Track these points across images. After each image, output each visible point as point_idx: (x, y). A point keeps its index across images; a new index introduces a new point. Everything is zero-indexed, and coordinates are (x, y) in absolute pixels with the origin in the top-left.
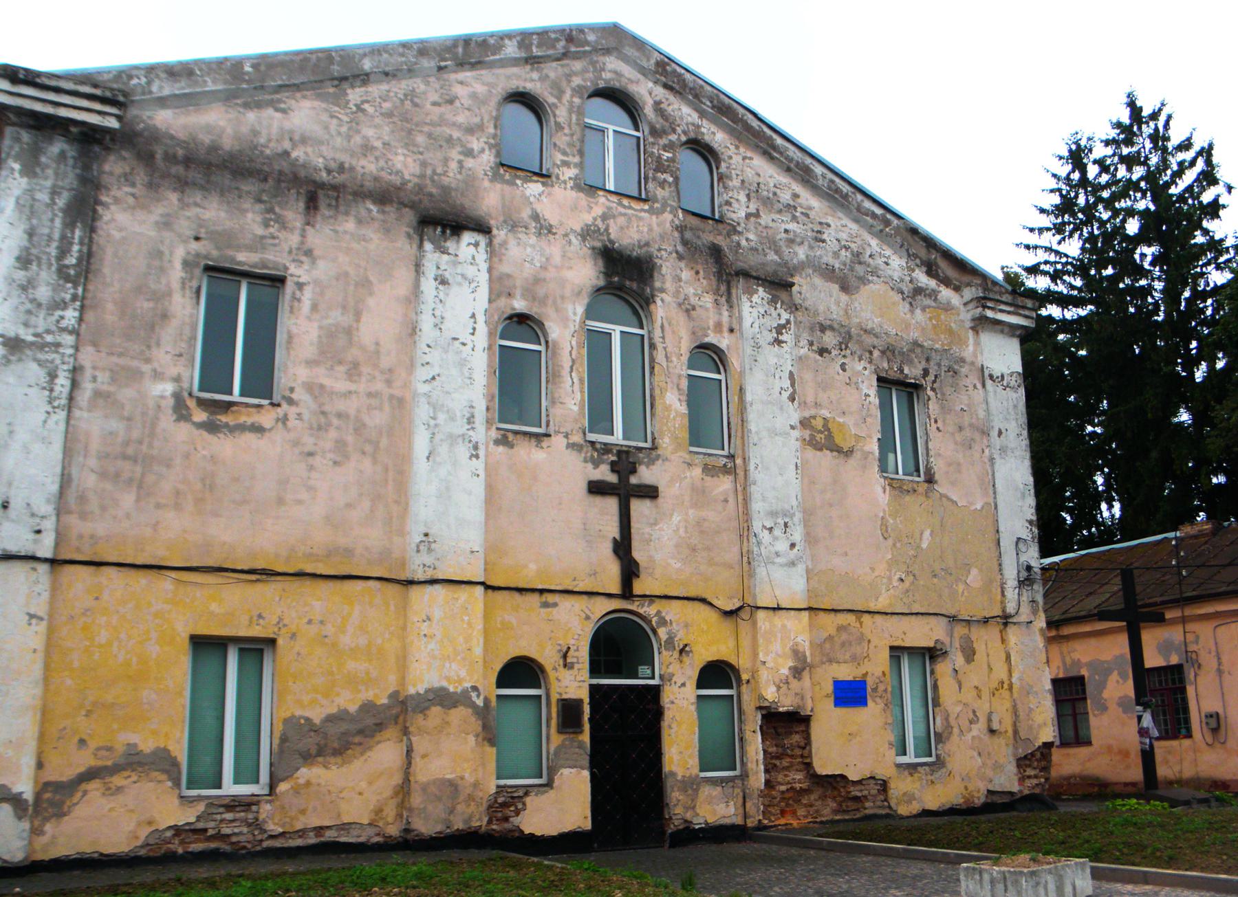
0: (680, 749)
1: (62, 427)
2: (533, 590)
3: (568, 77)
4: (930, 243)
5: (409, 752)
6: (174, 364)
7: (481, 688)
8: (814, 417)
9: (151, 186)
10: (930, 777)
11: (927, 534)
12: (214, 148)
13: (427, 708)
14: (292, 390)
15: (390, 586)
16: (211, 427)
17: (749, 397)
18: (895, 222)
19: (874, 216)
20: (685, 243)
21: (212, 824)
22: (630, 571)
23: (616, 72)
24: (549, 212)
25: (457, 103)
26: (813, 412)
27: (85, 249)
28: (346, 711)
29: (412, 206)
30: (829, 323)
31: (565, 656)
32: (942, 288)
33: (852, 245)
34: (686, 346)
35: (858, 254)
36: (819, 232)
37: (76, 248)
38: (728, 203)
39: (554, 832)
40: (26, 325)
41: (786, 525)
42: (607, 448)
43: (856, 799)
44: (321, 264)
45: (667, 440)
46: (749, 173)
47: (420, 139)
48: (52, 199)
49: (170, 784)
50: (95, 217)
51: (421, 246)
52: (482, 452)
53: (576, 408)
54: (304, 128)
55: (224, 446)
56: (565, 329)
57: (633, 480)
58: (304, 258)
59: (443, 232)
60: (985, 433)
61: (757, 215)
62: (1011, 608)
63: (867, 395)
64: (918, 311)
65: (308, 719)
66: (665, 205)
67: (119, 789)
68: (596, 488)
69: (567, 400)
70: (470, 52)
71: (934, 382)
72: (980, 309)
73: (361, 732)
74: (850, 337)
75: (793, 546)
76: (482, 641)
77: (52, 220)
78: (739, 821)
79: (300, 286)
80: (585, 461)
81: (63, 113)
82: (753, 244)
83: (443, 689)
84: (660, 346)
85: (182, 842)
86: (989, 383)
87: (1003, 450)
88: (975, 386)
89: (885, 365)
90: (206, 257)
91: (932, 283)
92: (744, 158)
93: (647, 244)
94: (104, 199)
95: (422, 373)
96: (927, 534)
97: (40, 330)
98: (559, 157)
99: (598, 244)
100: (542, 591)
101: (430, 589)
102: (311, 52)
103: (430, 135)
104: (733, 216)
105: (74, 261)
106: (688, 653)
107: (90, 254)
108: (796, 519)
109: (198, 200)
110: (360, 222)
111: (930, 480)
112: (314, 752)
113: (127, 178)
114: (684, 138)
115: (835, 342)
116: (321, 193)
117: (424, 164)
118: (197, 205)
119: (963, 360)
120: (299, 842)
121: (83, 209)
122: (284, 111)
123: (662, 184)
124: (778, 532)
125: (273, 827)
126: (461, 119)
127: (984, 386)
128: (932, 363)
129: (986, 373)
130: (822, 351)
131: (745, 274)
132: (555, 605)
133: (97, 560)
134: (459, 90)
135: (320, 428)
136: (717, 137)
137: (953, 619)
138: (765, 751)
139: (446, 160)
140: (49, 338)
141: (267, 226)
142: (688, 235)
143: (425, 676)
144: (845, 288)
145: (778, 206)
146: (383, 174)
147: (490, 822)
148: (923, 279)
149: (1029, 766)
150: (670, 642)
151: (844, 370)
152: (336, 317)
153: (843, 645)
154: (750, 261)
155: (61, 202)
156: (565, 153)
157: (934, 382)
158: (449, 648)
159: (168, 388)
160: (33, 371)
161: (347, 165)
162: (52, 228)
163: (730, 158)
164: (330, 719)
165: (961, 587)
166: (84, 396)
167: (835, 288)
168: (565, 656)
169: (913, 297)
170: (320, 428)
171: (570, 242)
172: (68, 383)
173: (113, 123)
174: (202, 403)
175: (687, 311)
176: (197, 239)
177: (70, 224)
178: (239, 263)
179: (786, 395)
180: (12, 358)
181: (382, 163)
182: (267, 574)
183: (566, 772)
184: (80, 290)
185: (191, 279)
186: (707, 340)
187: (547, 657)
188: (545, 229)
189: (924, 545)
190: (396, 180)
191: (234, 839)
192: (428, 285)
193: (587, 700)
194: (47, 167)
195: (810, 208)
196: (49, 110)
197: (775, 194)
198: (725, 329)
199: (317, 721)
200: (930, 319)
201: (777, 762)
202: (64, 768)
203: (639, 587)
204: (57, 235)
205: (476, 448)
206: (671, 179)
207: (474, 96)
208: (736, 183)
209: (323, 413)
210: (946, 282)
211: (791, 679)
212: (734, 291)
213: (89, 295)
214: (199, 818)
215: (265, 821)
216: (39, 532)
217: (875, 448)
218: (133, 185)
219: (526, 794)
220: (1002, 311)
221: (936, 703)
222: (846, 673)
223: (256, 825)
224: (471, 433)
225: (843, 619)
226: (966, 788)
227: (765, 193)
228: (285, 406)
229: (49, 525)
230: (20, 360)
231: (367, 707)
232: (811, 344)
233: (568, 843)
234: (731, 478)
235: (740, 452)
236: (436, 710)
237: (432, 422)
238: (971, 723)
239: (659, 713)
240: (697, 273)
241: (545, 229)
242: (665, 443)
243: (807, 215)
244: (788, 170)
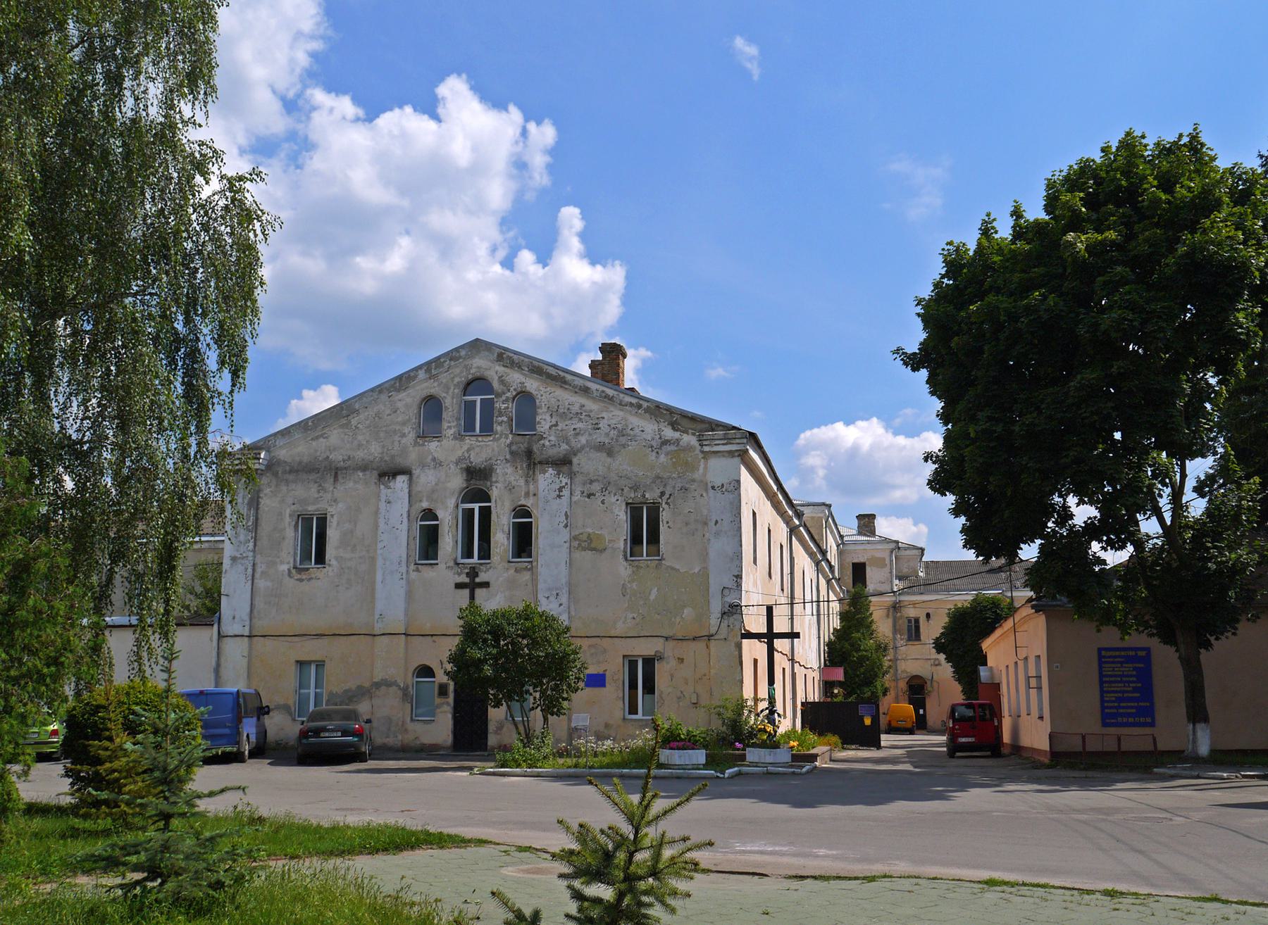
3: (452, 379)
4: (670, 410)
16: (301, 580)
19: (631, 404)
20: (512, 453)
24: (440, 455)
44: (340, 505)
47: (382, 435)
50: (258, 504)
54: (335, 444)
57: (477, 580)
60: (706, 524)
61: (556, 425)
68: (459, 586)
69: (449, 543)
70: (403, 381)
87: (717, 534)
91: (677, 435)
95: (380, 545)
107: (257, 519)
110: (355, 482)
113: (269, 485)
119: (694, 481)
123: (500, 423)
126: (400, 419)
130: (589, 496)
131: (540, 463)
134: (399, 404)
136: (532, 385)
142: (514, 448)
144: (610, 453)
148: (669, 433)
152: (347, 526)
154: (553, 452)
160: (240, 568)
165: (678, 619)
166: (257, 575)
188: (437, 463)
189: (652, 597)
192: (382, 505)
207: (406, 405)
210: (686, 432)
229: (247, 623)
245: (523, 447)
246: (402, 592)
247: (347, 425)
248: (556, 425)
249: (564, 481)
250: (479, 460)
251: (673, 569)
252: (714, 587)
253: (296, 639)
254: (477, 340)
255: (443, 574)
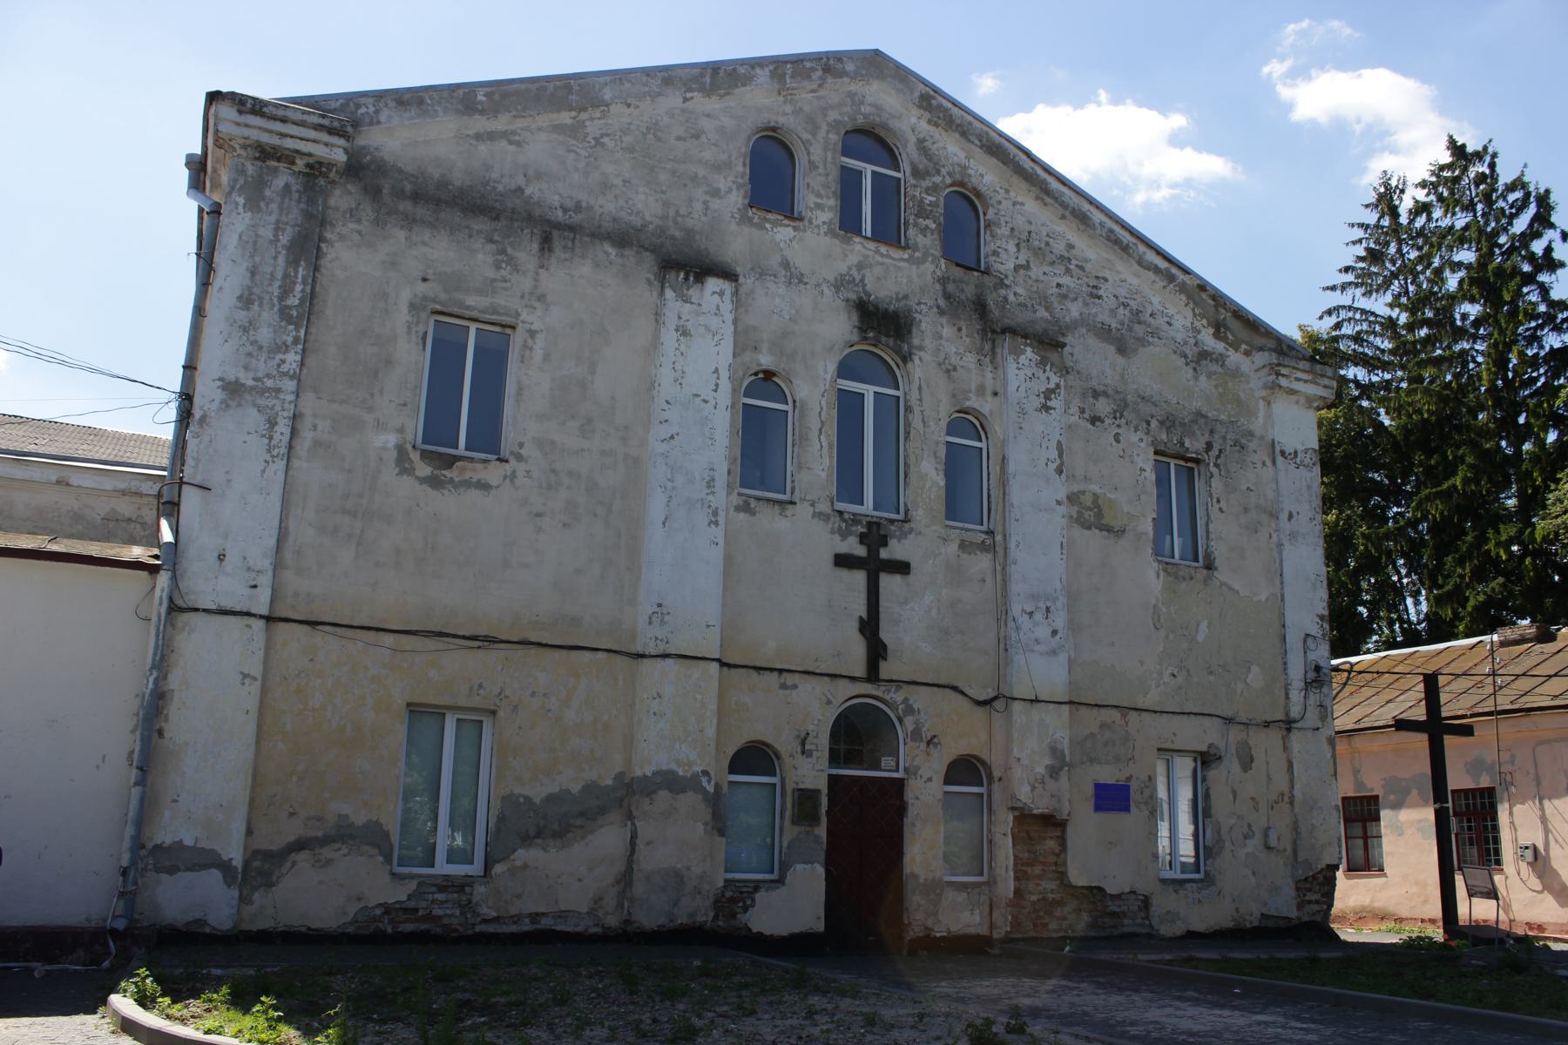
0: (927, 848)
1: (281, 475)
2: (771, 670)
4: (1219, 299)
5: (634, 836)
6: (397, 416)
7: (712, 774)
8: (1083, 493)
9: (376, 222)
10: (1197, 896)
11: (1204, 625)
12: (443, 183)
13: (654, 792)
14: (521, 445)
15: (619, 658)
16: (435, 482)
17: (1011, 468)
18: (1181, 276)
19: (1157, 270)
20: (947, 296)
21: (423, 904)
22: (877, 652)
23: (876, 106)
25: (703, 139)
26: (1082, 487)
27: (308, 289)
28: (568, 791)
29: (653, 250)
30: (1102, 388)
31: (803, 743)
32: (1231, 352)
33: (1132, 303)
34: (945, 411)
35: (1138, 312)
36: (1095, 287)
37: (299, 288)
38: (995, 253)
39: (784, 933)
40: (246, 368)
41: (1048, 610)
42: (855, 519)
43: (1114, 914)
45: (921, 512)
46: (1020, 221)
48: (276, 235)
49: (381, 859)
50: (319, 255)
51: (662, 293)
52: (721, 519)
53: (823, 475)
54: (538, 162)
55: (447, 503)
56: (813, 391)
57: (884, 554)
58: (537, 304)
59: (686, 279)
60: (1274, 516)
61: (1027, 267)
62: (1295, 712)
63: (1142, 470)
64: (1203, 378)
65: (527, 798)
66: (926, 254)
67: (329, 862)
68: (843, 561)
69: (814, 464)
71: (1218, 457)
72: (1273, 377)
73: (582, 814)
74: (1126, 405)
75: (1054, 633)
76: (715, 721)
77: (275, 258)
78: (984, 931)
79: (532, 334)
80: (832, 532)
81: (289, 144)
82: (1021, 299)
83: (672, 772)
84: (917, 410)
85: (391, 921)
86: (1280, 459)
87: (1293, 536)
88: (1264, 463)
89: (1164, 437)
90: (434, 300)
91: (1220, 346)
92: (1014, 204)
93: (906, 297)
94: (328, 235)
96: (1204, 625)
97: (260, 374)
98: (812, 199)
99: (853, 296)
100: (781, 671)
101: (660, 663)
102: (548, 79)
103: (674, 173)
104: (1001, 268)
105: (297, 302)
106: (936, 745)
107: (313, 294)
108: (1059, 604)
109: (426, 238)
111: (1210, 566)
112: (532, 832)
113: (352, 213)
114: (948, 181)
115: (1108, 409)
116: (555, 234)
117: (666, 204)
118: (424, 243)
119: (1251, 434)
120: (513, 928)
121: (307, 247)
122: (518, 144)
123: (924, 231)
124: (1038, 616)
125: (487, 911)
126: (707, 155)
127: (1274, 463)
128: (1216, 436)
129: (1278, 449)
130: (1094, 420)
132: (795, 687)
133: (313, 619)
134: (705, 123)
135: (549, 488)
136: (986, 175)
137: (1229, 720)
138: (1016, 857)
139: (690, 200)
140: (269, 383)
141: (498, 267)
142: (951, 288)
143: (652, 758)
144: (1122, 350)
145: (1050, 258)
146: (623, 214)
147: (716, 917)
148: (1208, 340)
149: (1310, 890)
150: (916, 734)
151: (1118, 441)
153: (1106, 744)
154: (1021, 317)
155: (285, 239)
156: (819, 195)
157: (1218, 457)
158: (676, 728)
159: (391, 439)
160: (253, 418)
161: (584, 204)
162: (275, 267)
163: (1000, 203)
164: (550, 799)
167: (1112, 349)
168: (803, 743)
169: (1197, 362)
170: (549, 488)
171: (822, 293)
172: (287, 431)
173: (340, 157)
174: (425, 455)
175: (948, 371)
176: (424, 280)
177: (293, 262)
178: (468, 308)
179: (1053, 466)
180: (233, 404)
181: (621, 202)
182: (490, 640)
183: (800, 867)
184: (302, 332)
185: (418, 323)
186: (968, 404)
187: (784, 743)
188: (795, 278)
190: (638, 222)
191: (446, 921)
192: (669, 336)
193: (825, 791)
194: (271, 201)
195: (1086, 261)
196: (275, 141)
197: (1047, 244)
198: (989, 392)
199: (537, 801)
200: (1216, 386)
201: (1029, 870)
202: (275, 836)
203: (886, 669)
204: (279, 274)
205: (715, 514)
206: (933, 226)
207: (721, 130)
208: (1003, 231)
209: (553, 471)
211: (1047, 779)
212: (998, 351)
213: (311, 338)
214: (410, 897)
215: (477, 904)
216: (255, 586)
217: (1148, 527)
218: (359, 221)
219: (756, 889)
220: (1298, 379)
221: (1207, 813)
222: (1108, 775)
223: (468, 907)
224: (710, 497)
225: (1106, 715)
226: (1237, 910)
227: (1036, 243)
228: (513, 461)
229: (265, 581)
230: (239, 405)
231: (590, 788)
232: (1082, 411)
233: (798, 945)
234: (990, 556)
235: (1000, 529)
236: (663, 795)
237: (669, 485)
238: (1245, 837)
239: (901, 809)
240: (960, 330)
241: (795, 278)
242: (919, 515)
243: (1081, 268)
244: (1063, 217)
245: (970, 291)
246: (716, 555)
247: (575, 130)
248: (1027, 267)
249: (1055, 379)
250: (882, 294)
251: (1230, 588)
252: (1294, 639)
253: (431, 644)
254: (877, 52)
255: (806, 537)
